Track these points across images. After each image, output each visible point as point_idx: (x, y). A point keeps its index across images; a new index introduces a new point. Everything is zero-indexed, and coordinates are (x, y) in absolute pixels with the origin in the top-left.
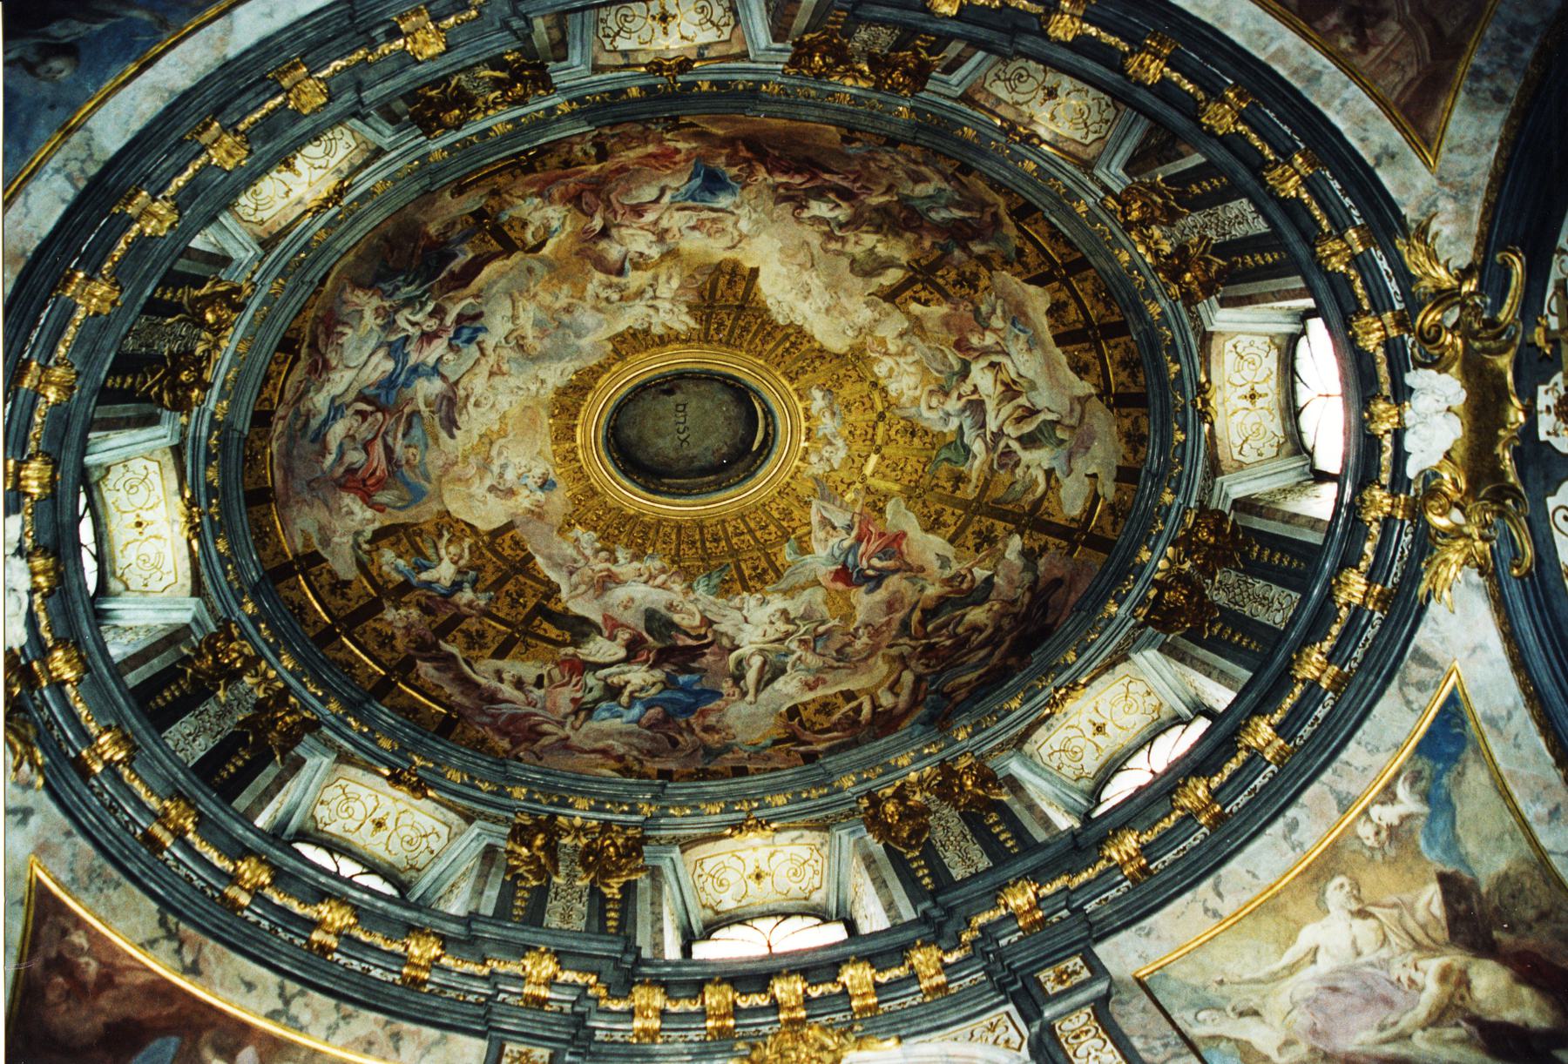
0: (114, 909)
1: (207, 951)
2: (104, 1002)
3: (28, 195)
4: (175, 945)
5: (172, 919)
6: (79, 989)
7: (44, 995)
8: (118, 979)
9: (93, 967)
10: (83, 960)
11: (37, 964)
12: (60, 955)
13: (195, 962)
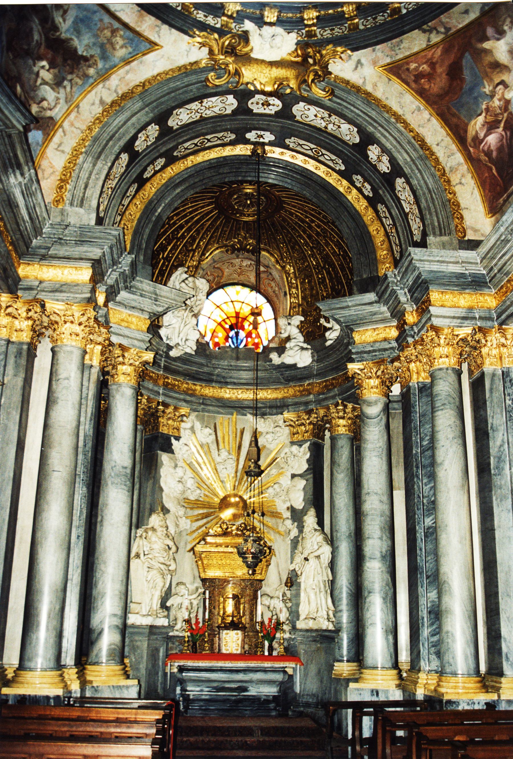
0: (409, 48)
1: (444, 20)
2: (439, 70)
3: (115, 10)
4: (435, 32)
5: (425, 27)
6: (430, 77)
7: (425, 89)
8: (434, 60)
9: (425, 67)
10: (421, 69)
11: (414, 85)
12: (415, 76)
13: (445, 28)
